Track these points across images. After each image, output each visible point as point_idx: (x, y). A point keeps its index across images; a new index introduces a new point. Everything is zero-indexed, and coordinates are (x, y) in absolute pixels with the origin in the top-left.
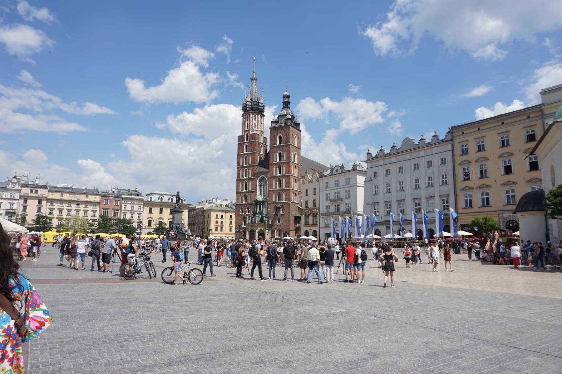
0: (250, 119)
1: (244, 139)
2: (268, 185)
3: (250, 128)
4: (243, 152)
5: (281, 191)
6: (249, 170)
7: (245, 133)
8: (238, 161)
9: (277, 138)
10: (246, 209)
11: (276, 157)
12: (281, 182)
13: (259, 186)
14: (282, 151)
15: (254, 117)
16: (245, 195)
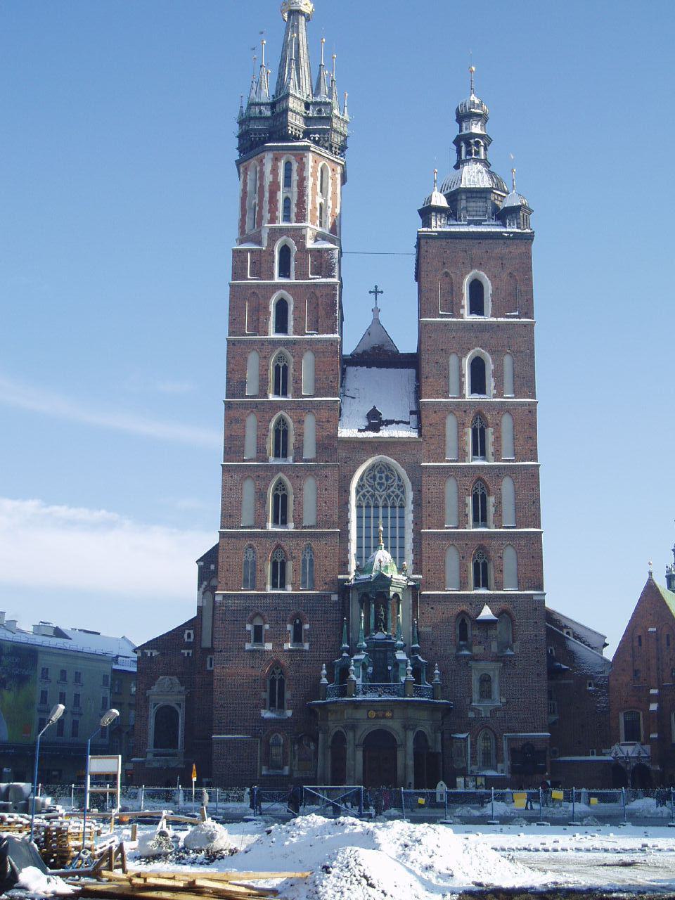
0: (302, 180)
1: (272, 269)
2: (417, 503)
3: (301, 217)
4: (259, 328)
5: (495, 544)
6: (300, 422)
7: (272, 240)
8: (230, 372)
9: (460, 288)
10: (285, 622)
11: (464, 376)
12: (491, 500)
13: (359, 507)
14: (491, 352)
15: (319, 174)
16: (278, 546)
